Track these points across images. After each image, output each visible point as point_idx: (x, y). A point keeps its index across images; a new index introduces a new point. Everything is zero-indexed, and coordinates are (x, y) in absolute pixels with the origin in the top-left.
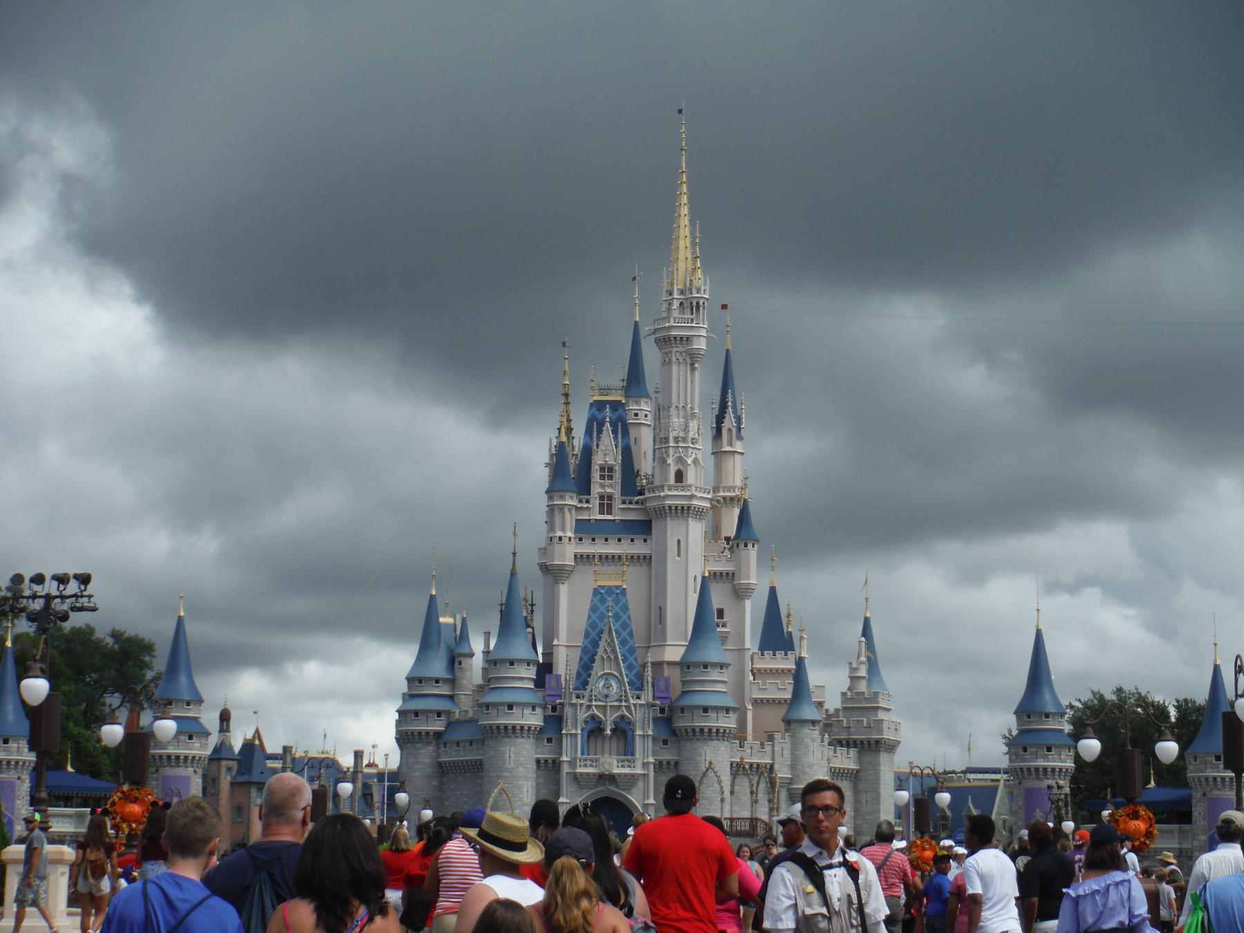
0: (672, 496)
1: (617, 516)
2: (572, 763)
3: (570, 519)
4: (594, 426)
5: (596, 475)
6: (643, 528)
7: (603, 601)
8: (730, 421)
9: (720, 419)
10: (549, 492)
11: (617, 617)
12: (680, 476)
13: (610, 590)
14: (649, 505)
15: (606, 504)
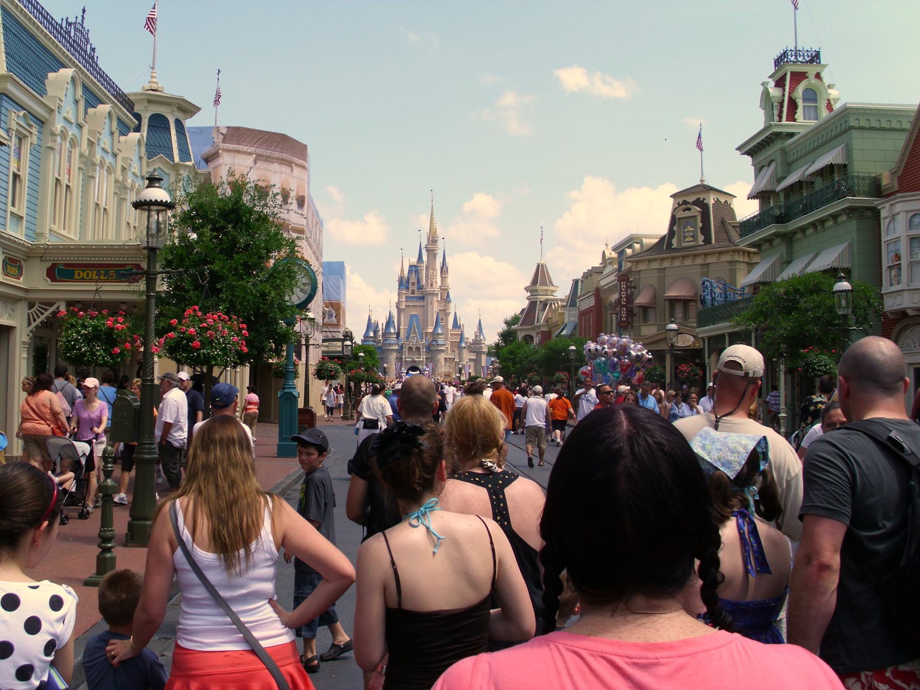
0: (429, 289)
1: (416, 295)
2: (405, 358)
3: (404, 297)
4: (410, 272)
5: (410, 284)
6: (423, 298)
7: (413, 318)
8: (445, 269)
9: (442, 268)
10: (399, 289)
11: (416, 322)
12: (432, 285)
13: (414, 315)
14: (424, 292)
15: (413, 292)
